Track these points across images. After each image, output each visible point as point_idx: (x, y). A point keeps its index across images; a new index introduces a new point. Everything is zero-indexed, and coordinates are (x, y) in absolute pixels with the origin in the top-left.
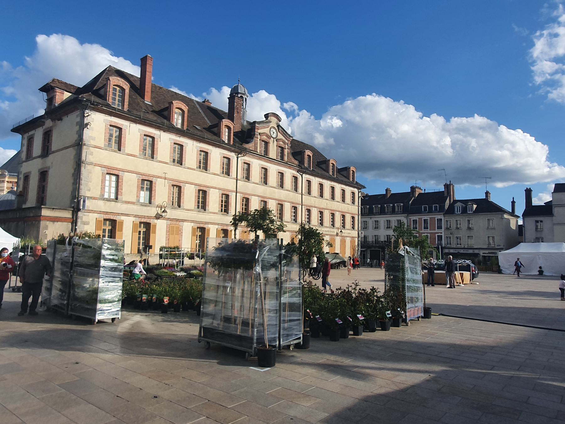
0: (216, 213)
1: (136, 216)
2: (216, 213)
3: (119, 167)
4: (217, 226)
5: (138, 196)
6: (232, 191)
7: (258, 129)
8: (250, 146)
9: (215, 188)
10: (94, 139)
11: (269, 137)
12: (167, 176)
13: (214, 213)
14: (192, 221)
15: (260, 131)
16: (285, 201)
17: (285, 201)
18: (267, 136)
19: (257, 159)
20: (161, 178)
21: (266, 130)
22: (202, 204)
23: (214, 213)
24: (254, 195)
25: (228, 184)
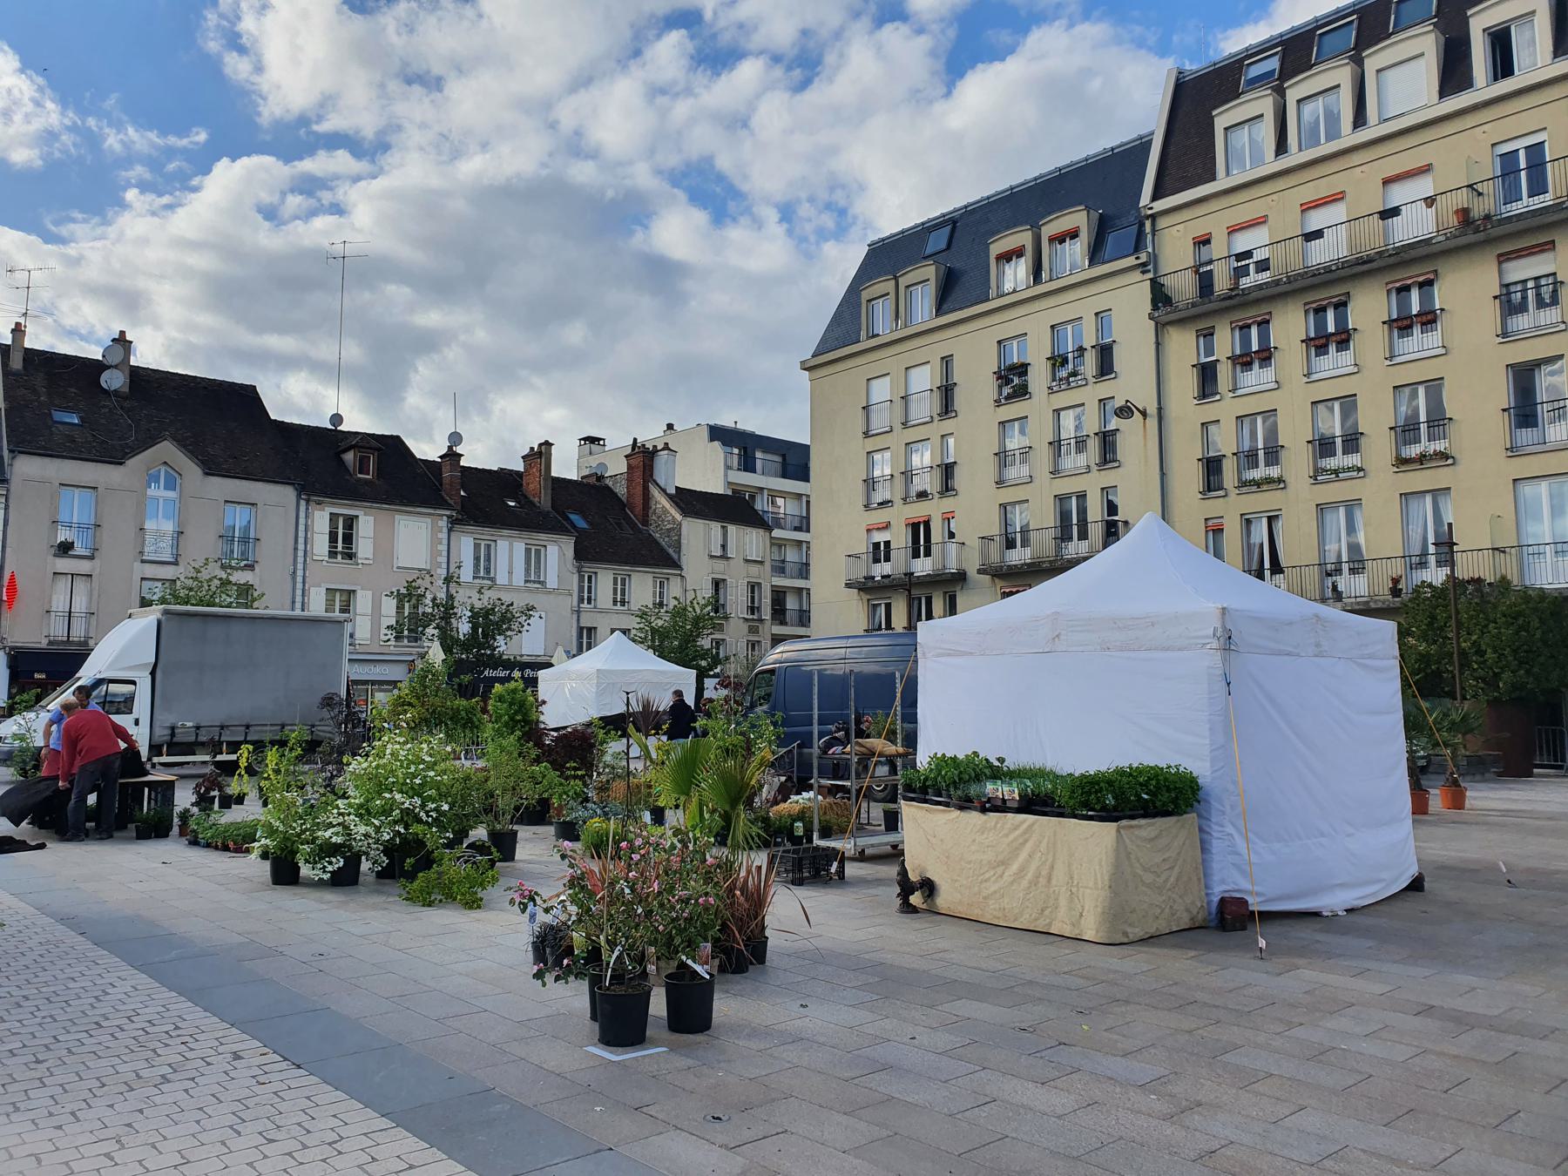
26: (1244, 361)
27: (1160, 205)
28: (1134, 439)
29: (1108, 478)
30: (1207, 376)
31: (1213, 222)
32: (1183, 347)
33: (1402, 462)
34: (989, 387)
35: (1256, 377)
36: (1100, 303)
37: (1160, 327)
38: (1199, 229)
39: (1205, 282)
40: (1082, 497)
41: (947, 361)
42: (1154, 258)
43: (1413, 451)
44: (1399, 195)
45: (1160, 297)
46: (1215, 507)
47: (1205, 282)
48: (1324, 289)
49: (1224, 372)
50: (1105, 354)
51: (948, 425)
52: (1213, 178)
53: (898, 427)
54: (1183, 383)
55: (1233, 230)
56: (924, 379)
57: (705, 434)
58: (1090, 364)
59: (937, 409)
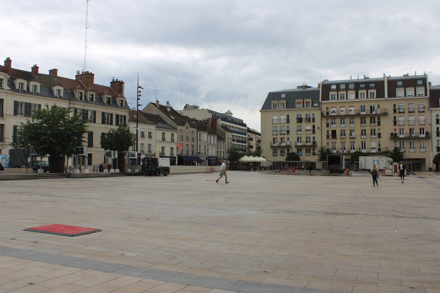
26: (332, 123)
27: (323, 102)
28: (317, 130)
29: (314, 135)
30: (328, 125)
31: (329, 106)
32: (325, 122)
33: (350, 138)
34: (295, 121)
35: (333, 126)
36: (313, 112)
37: (322, 117)
38: (327, 106)
39: (328, 113)
40: (310, 137)
41: (288, 116)
42: (321, 108)
43: (351, 137)
44: (351, 108)
45: (322, 114)
46: (328, 141)
47: (328, 113)
48: (342, 118)
49: (330, 124)
50: (314, 120)
51: (288, 125)
52: (329, 100)
53: (279, 123)
54: (324, 125)
55: (331, 107)
56: (284, 117)
57: (207, 111)
58: (311, 120)
59: (286, 122)
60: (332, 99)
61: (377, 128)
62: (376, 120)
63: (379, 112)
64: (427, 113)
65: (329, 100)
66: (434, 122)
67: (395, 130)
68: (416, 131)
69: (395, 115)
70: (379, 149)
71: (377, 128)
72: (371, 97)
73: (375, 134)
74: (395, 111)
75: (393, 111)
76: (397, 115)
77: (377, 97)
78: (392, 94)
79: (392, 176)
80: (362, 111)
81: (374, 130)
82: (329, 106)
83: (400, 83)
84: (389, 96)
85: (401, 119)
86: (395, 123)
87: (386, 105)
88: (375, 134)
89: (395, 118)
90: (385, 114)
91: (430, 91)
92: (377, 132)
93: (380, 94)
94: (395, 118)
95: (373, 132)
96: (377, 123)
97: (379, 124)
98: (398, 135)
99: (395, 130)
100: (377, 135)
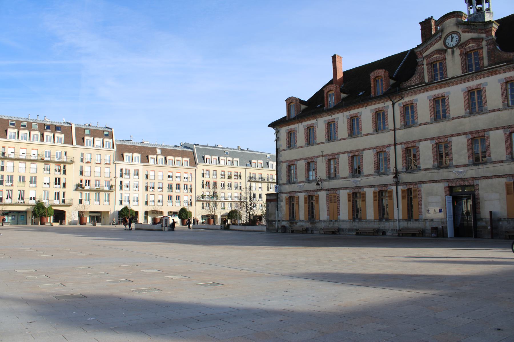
0: (372, 175)
1: (305, 191)
2: (372, 175)
3: (312, 155)
4: (373, 189)
5: (308, 176)
6: (389, 146)
7: (421, 54)
8: (414, 80)
9: (368, 149)
10: (281, 146)
11: (442, 51)
12: (324, 153)
13: (369, 175)
14: (347, 188)
15: (424, 55)
16: (488, 130)
17: (488, 130)
18: (439, 51)
19: (424, 92)
20: (319, 156)
21: (439, 45)
22: (356, 171)
23: (369, 175)
24: (423, 140)
25: (385, 139)
31: (7, 145)
52: (6, 138)
60: (10, 138)
61: (62, 177)
62: (62, 168)
63: (65, 160)
64: (113, 166)
65: (6, 138)
66: (118, 175)
67: (81, 181)
68: (103, 183)
69: (82, 164)
70: (64, 201)
71: (62, 177)
72: (58, 142)
73: (59, 184)
74: (82, 160)
75: (80, 160)
76: (84, 164)
77: (65, 143)
78: (81, 141)
79: (162, 230)
80: (46, 156)
81: (59, 179)
82: (7, 145)
83: (87, 132)
84: (78, 144)
85: (87, 169)
86: (81, 173)
87: (74, 152)
88: (59, 184)
89: (82, 167)
90: (71, 162)
91: (116, 144)
92: (62, 181)
93: (68, 141)
94: (82, 167)
95: (57, 181)
96: (62, 171)
97: (65, 172)
98: (84, 185)
99: (81, 181)
100: (62, 185)
